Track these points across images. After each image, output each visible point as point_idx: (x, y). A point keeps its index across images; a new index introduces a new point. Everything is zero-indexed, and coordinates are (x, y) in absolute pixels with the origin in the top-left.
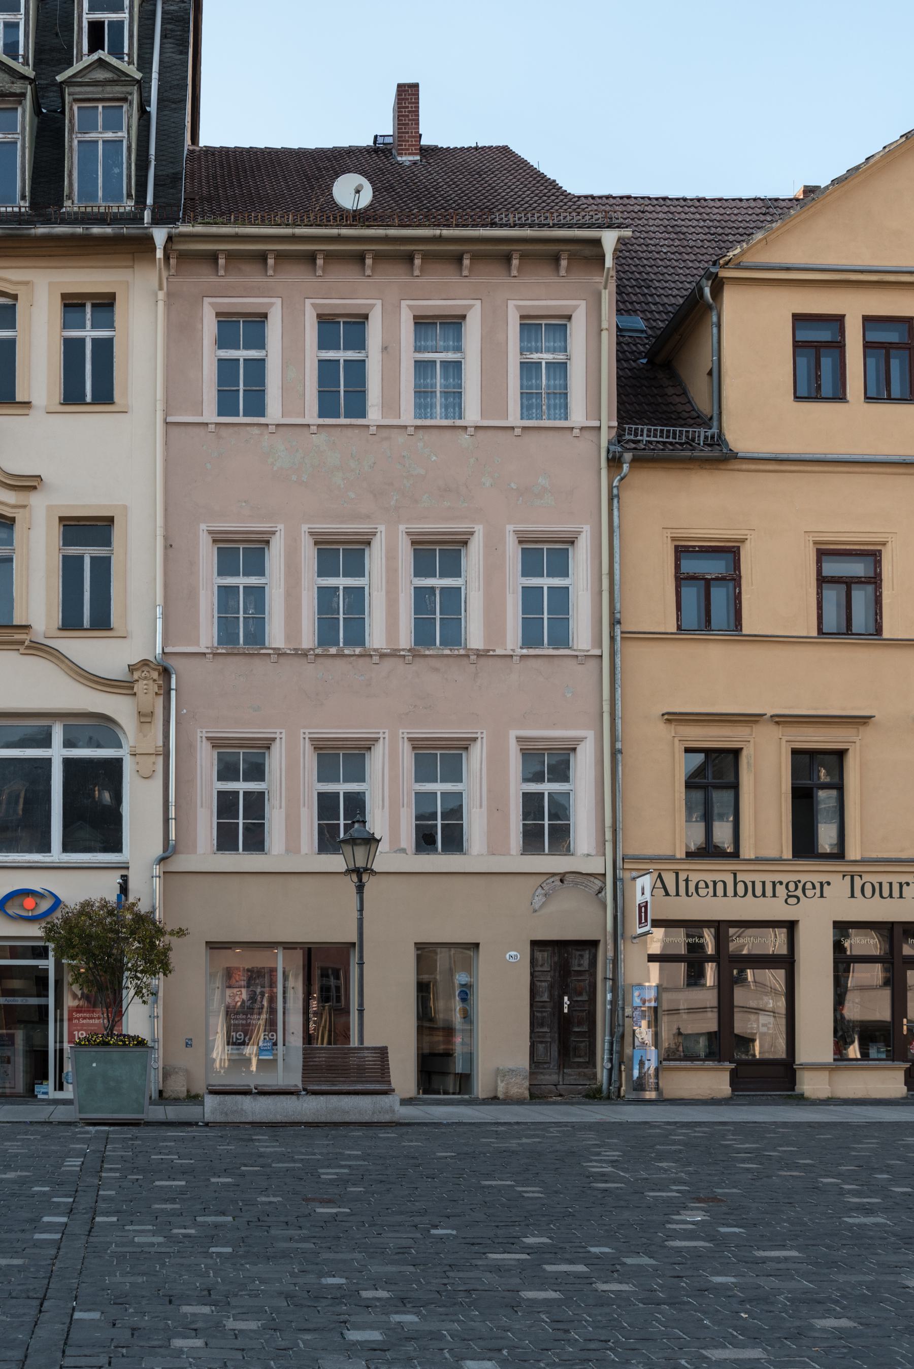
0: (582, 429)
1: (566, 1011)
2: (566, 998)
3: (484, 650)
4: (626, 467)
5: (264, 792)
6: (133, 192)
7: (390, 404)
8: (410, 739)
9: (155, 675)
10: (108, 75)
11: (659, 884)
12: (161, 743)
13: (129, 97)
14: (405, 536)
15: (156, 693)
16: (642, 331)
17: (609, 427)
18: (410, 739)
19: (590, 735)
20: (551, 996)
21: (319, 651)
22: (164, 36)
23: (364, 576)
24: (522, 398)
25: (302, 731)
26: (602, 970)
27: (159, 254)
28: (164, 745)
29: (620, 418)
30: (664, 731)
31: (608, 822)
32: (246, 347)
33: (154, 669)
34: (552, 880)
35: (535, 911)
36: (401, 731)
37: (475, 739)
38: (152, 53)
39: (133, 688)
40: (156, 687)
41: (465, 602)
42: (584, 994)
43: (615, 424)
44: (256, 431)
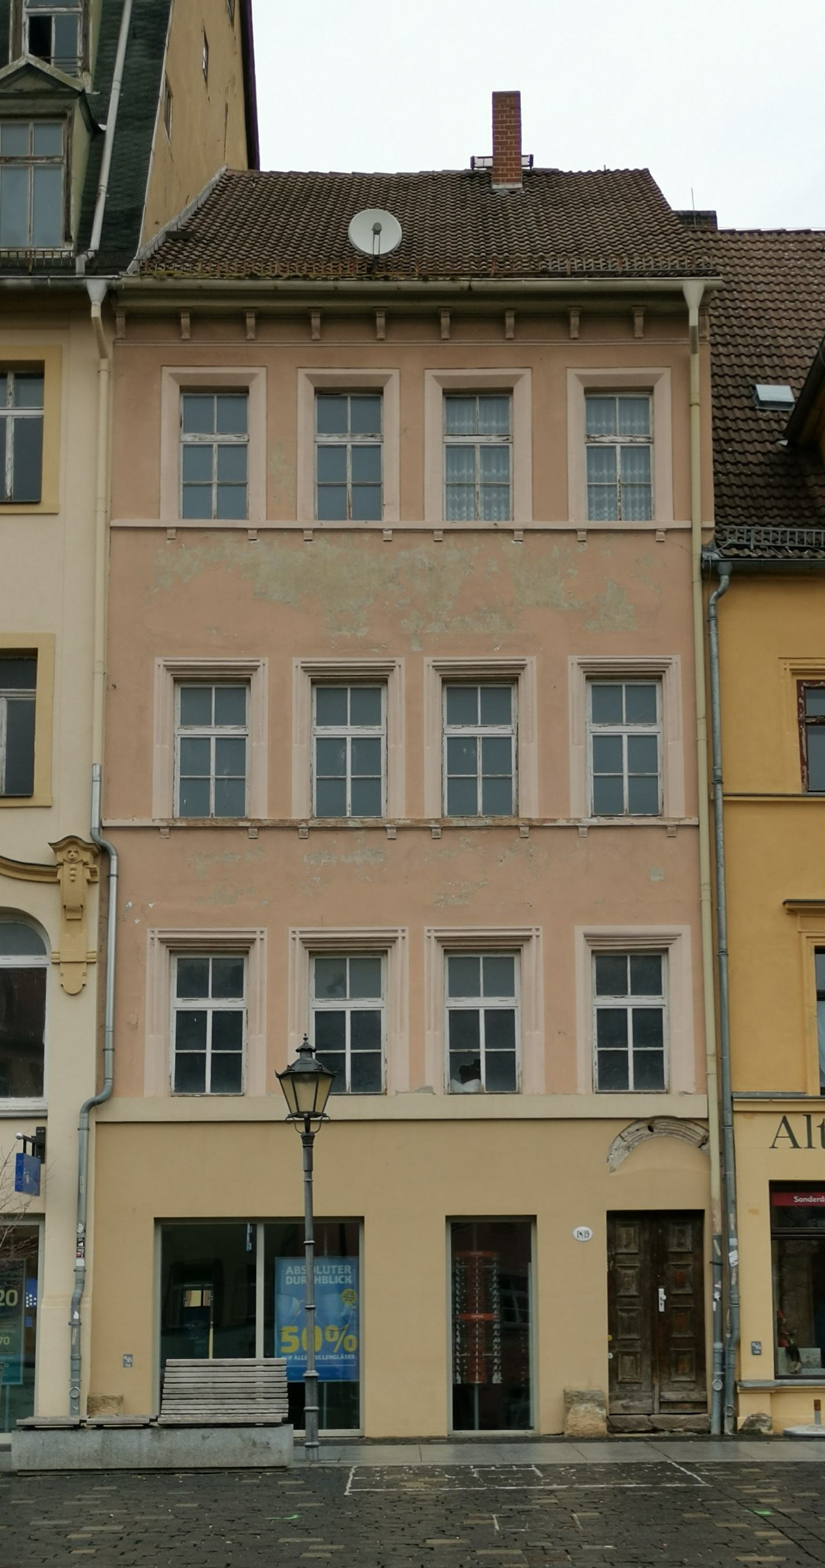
0: (668, 531)
3: (537, 820)
4: (725, 579)
5: (241, 1013)
6: (73, 233)
7: (413, 501)
8: (439, 939)
9: (87, 857)
10: (41, 85)
11: (784, 1132)
12: (94, 946)
13: (69, 113)
14: (432, 671)
15: (89, 882)
16: (789, 404)
17: (703, 529)
18: (439, 939)
19: (685, 930)
21: (312, 823)
22: (132, 35)
23: (380, 724)
24: (589, 493)
25: (291, 929)
26: (710, 1249)
27: (96, 312)
28: (100, 950)
29: (721, 515)
32: (222, 431)
33: (85, 849)
34: (636, 1127)
35: (613, 1170)
36: (426, 928)
37: (528, 938)
38: (115, 57)
39: (55, 874)
40: (88, 872)
41: (517, 756)
43: (711, 524)
44: (229, 538)
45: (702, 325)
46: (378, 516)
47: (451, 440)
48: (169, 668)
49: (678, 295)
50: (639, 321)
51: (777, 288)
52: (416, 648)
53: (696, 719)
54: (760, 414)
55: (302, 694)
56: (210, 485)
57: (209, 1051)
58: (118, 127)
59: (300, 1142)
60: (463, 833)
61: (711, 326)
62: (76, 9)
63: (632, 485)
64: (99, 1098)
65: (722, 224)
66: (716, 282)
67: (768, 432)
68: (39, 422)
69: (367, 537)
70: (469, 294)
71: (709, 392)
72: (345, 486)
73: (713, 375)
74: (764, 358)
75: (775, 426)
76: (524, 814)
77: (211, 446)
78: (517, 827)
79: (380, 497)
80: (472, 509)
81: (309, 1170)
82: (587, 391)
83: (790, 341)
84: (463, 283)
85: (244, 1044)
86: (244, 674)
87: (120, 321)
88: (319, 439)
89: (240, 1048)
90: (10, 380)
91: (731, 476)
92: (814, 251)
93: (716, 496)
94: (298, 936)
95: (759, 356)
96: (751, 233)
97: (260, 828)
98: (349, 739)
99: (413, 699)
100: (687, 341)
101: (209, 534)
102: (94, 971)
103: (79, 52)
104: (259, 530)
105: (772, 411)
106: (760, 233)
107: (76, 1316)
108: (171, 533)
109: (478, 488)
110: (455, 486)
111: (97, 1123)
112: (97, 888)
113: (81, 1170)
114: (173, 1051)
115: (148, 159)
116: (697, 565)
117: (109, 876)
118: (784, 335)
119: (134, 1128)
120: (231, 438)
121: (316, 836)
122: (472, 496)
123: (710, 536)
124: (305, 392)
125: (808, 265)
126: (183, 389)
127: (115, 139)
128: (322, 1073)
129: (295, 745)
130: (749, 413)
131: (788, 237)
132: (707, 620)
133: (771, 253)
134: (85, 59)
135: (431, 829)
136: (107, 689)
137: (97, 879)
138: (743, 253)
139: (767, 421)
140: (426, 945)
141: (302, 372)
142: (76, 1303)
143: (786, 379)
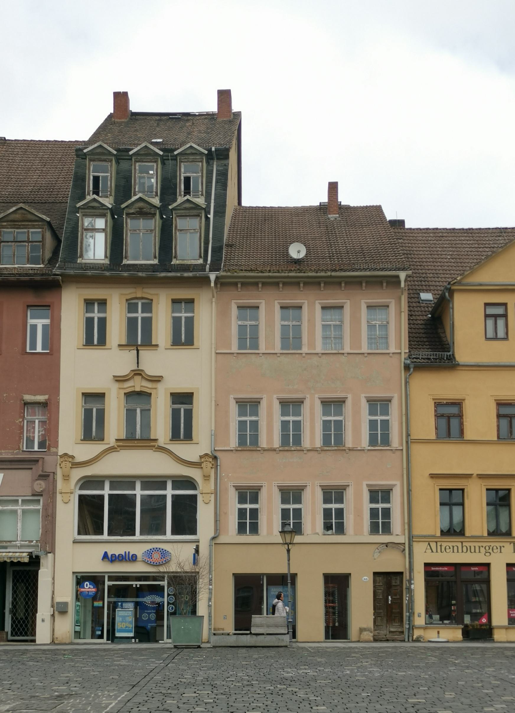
0: (393, 353)
1: (390, 603)
2: (390, 597)
3: (352, 448)
4: (412, 369)
5: (258, 509)
6: (202, 255)
7: (312, 344)
8: (320, 486)
9: (211, 460)
10: (191, 205)
11: (429, 547)
12: (213, 488)
13: (201, 215)
14: (318, 399)
15: (211, 468)
16: (431, 301)
17: (405, 353)
18: (320, 486)
19: (398, 483)
20: (383, 596)
21: (280, 449)
22: (217, 182)
23: (301, 416)
24: (368, 340)
25: (274, 482)
26: (405, 584)
27: (212, 284)
28: (215, 489)
29: (411, 347)
30: (430, 482)
31: (406, 521)
32: (250, 320)
33: (210, 457)
34: (382, 545)
35: (375, 559)
36: (316, 482)
37: (348, 486)
38: (211, 190)
39: (201, 465)
40: (211, 464)
41: (345, 427)
42: (398, 595)
43: (407, 351)
44: (253, 356)
45: (405, 286)
46: (300, 348)
47: (323, 323)
48: (235, 398)
49: (398, 277)
50: (385, 284)
51: (427, 253)
52: (313, 392)
53: (402, 415)
54: (422, 305)
55: (277, 407)
56: (247, 338)
57: (248, 521)
58: (214, 216)
59: (286, 552)
60: (328, 452)
61: (408, 285)
62: (199, 174)
63: (382, 338)
64: (215, 536)
65: (407, 226)
66: (410, 272)
67: (425, 312)
68: (192, 318)
69: (297, 356)
70: (331, 277)
71: (407, 308)
72: (290, 338)
73: (408, 302)
74: (423, 282)
75: (427, 309)
76: (347, 446)
77: (247, 325)
78: (345, 450)
79: (301, 342)
80: (330, 345)
81: (289, 560)
82: (368, 307)
83: (431, 275)
84: (329, 274)
85: (259, 519)
86: (258, 400)
87: (219, 286)
88: (281, 323)
89: (258, 520)
90: (183, 304)
91: (412, 329)
92: (439, 237)
93: (409, 345)
94: (276, 485)
95: (421, 281)
96: (417, 229)
97: (264, 450)
98: (291, 421)
99: (312, 408)
100: (400, 290)
101: (247, 355)
102: (213, 496)
103: (200, 189)
104: (263, 354)
105: (426, 303)
106: (420, 229)
107: (210, 603)
108: (235, 355)
109: (332, 339)
110: (325, 338)
111: (215, 544)
112: (213, 469)
113: (210, 558)
114: (237, 521)
115: (224, 227)
116: (403, 365)
117: (217, 466)
118: (429, 272)
119: (226, 545)
120: (253, 323)
121: (281, 453)
122: (330, 341)
123: (407, 355)
124: (277, 307)
125: (437, 243)
126: (238, 307)
127: (213, 220)
128: (293, 531)
129: (275, 424)
130: (418, 304)
131: (430, 231)
132: (406, 383)
133: (424, 238)
134: (202, 191)
135: (318, 450)
136: (216, 406)
137: (213, 467)
138: (415, 238)
139: (424, 307)
140: (316, 488)
141: (276, 301)
142: (210, 600)
143: (430, 290)
